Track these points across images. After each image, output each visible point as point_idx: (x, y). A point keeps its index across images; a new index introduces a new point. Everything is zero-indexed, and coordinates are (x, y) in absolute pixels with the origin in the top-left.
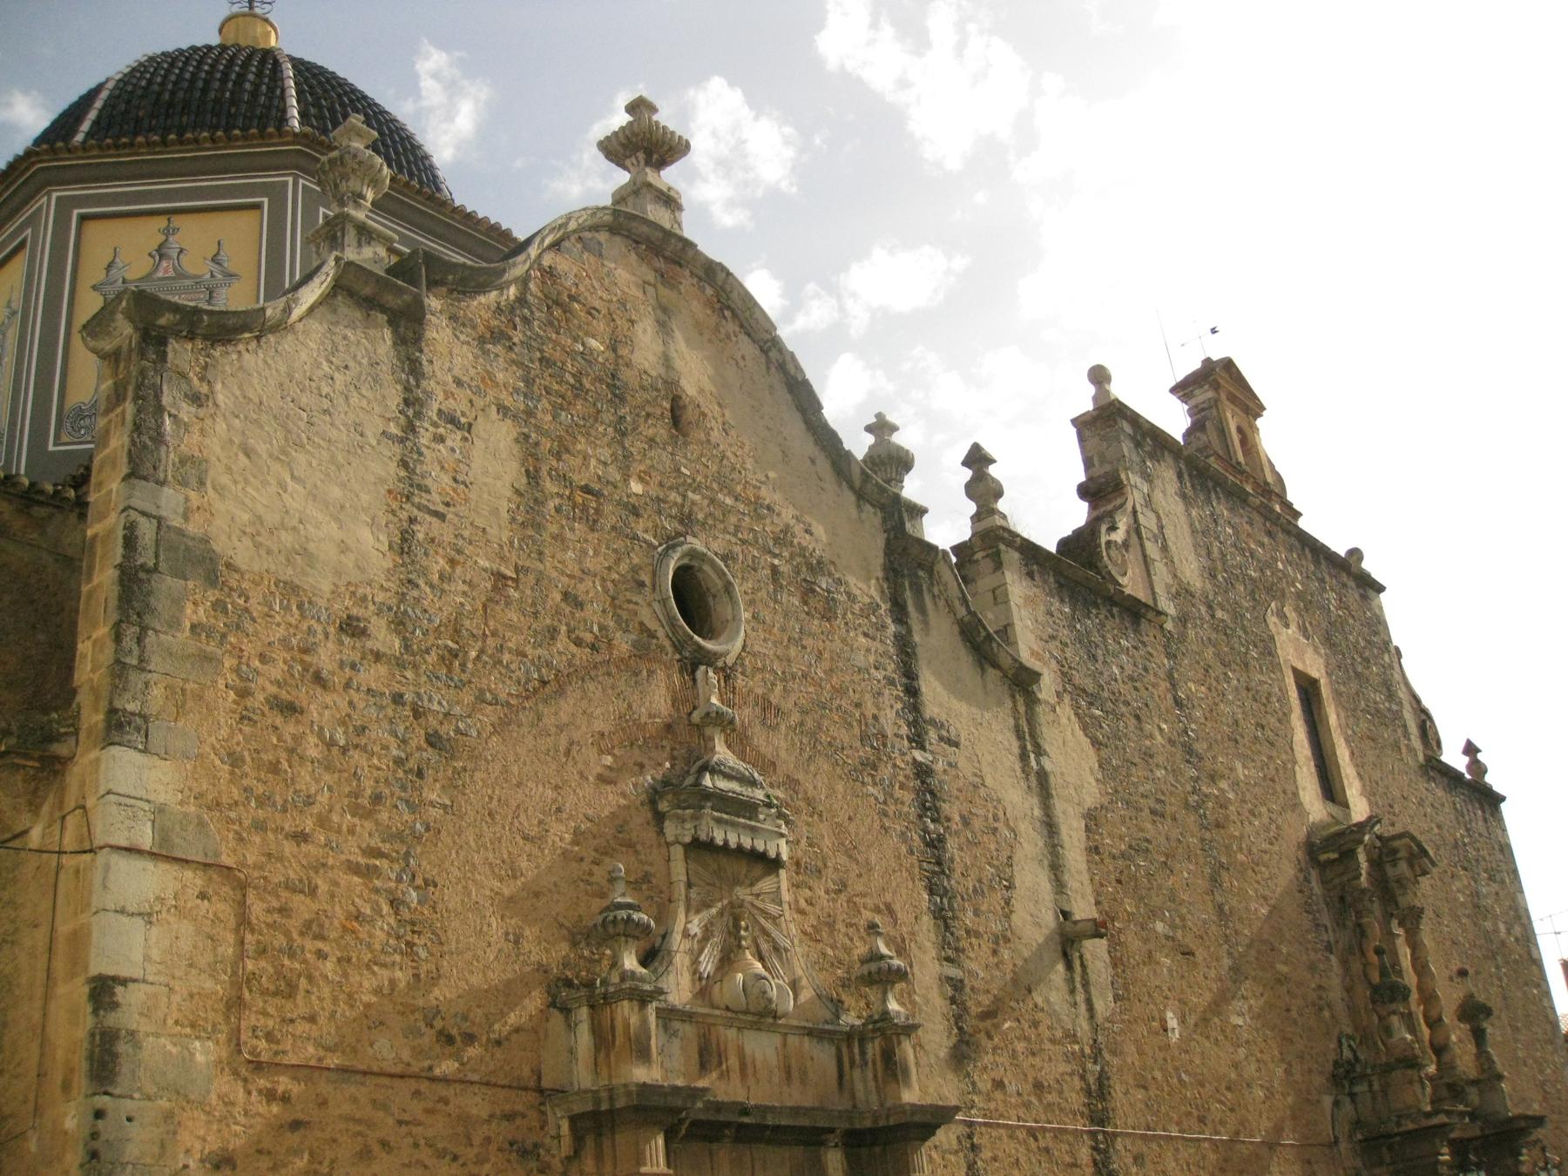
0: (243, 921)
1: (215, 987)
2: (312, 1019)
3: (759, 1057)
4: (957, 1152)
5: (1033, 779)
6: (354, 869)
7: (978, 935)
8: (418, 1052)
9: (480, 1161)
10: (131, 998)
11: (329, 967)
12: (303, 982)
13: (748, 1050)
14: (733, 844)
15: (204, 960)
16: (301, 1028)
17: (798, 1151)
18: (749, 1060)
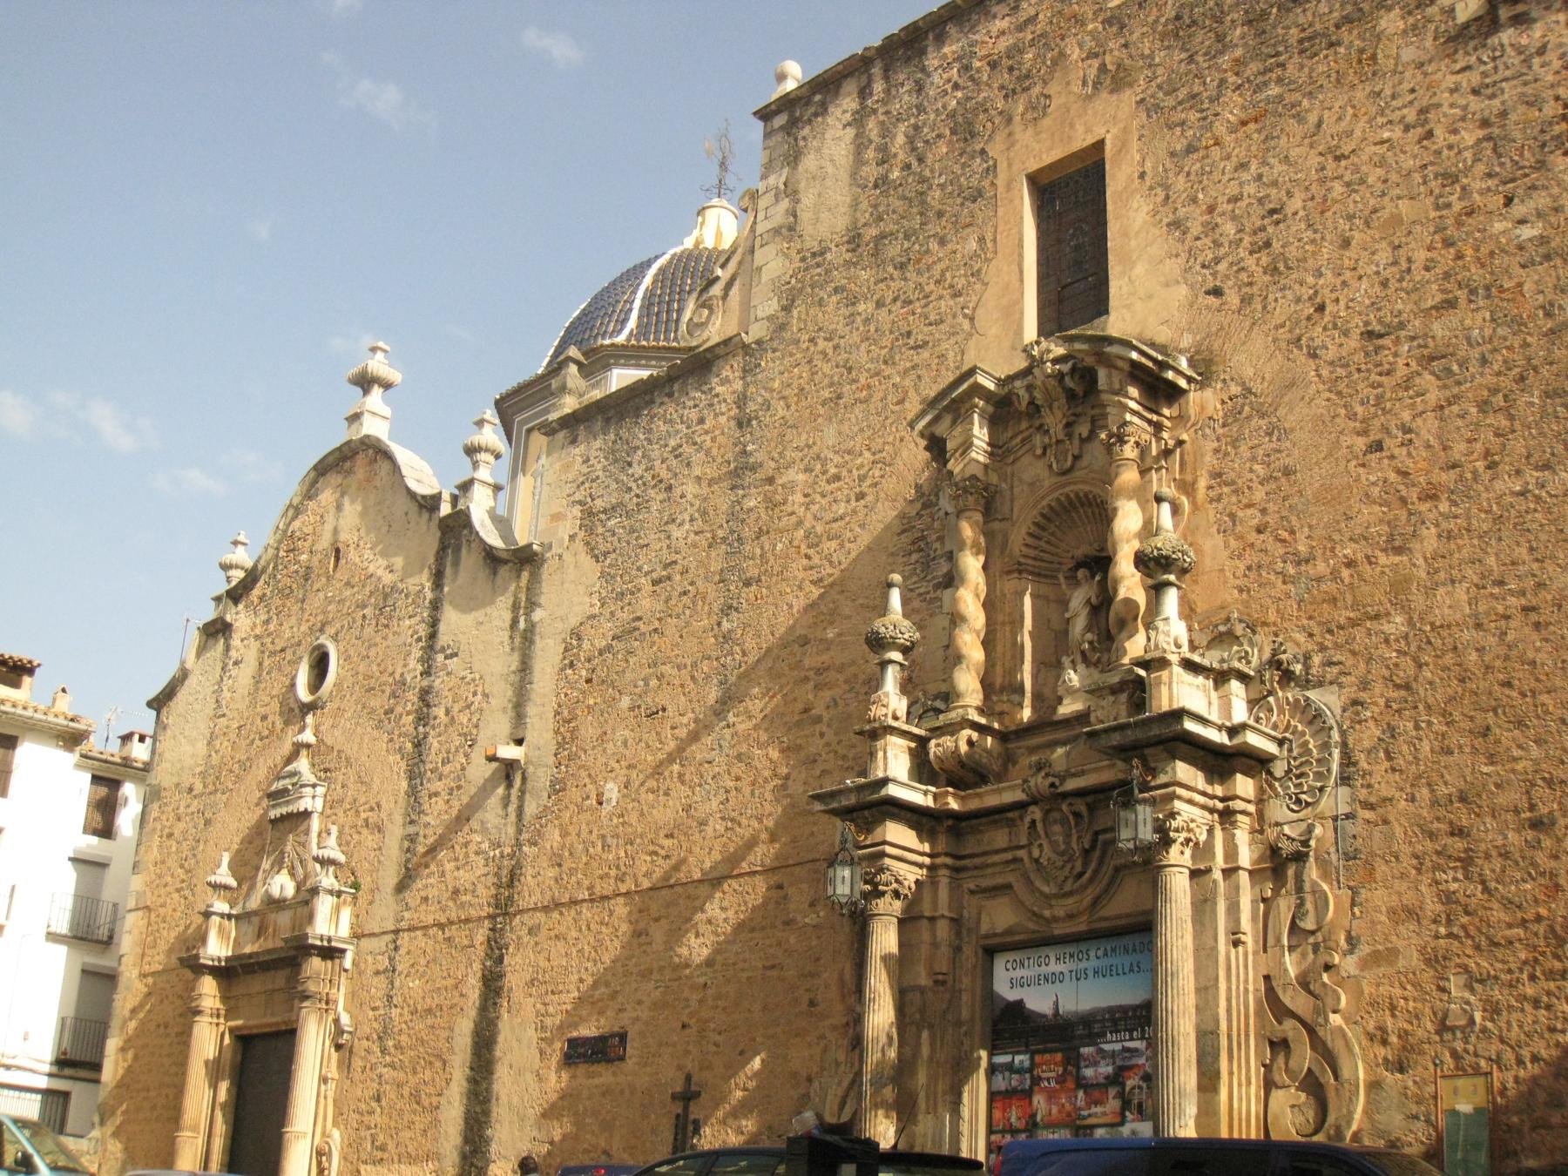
0: (149, 924)
1: (140, 951)
5: (518, 640)
6: (178, 890)
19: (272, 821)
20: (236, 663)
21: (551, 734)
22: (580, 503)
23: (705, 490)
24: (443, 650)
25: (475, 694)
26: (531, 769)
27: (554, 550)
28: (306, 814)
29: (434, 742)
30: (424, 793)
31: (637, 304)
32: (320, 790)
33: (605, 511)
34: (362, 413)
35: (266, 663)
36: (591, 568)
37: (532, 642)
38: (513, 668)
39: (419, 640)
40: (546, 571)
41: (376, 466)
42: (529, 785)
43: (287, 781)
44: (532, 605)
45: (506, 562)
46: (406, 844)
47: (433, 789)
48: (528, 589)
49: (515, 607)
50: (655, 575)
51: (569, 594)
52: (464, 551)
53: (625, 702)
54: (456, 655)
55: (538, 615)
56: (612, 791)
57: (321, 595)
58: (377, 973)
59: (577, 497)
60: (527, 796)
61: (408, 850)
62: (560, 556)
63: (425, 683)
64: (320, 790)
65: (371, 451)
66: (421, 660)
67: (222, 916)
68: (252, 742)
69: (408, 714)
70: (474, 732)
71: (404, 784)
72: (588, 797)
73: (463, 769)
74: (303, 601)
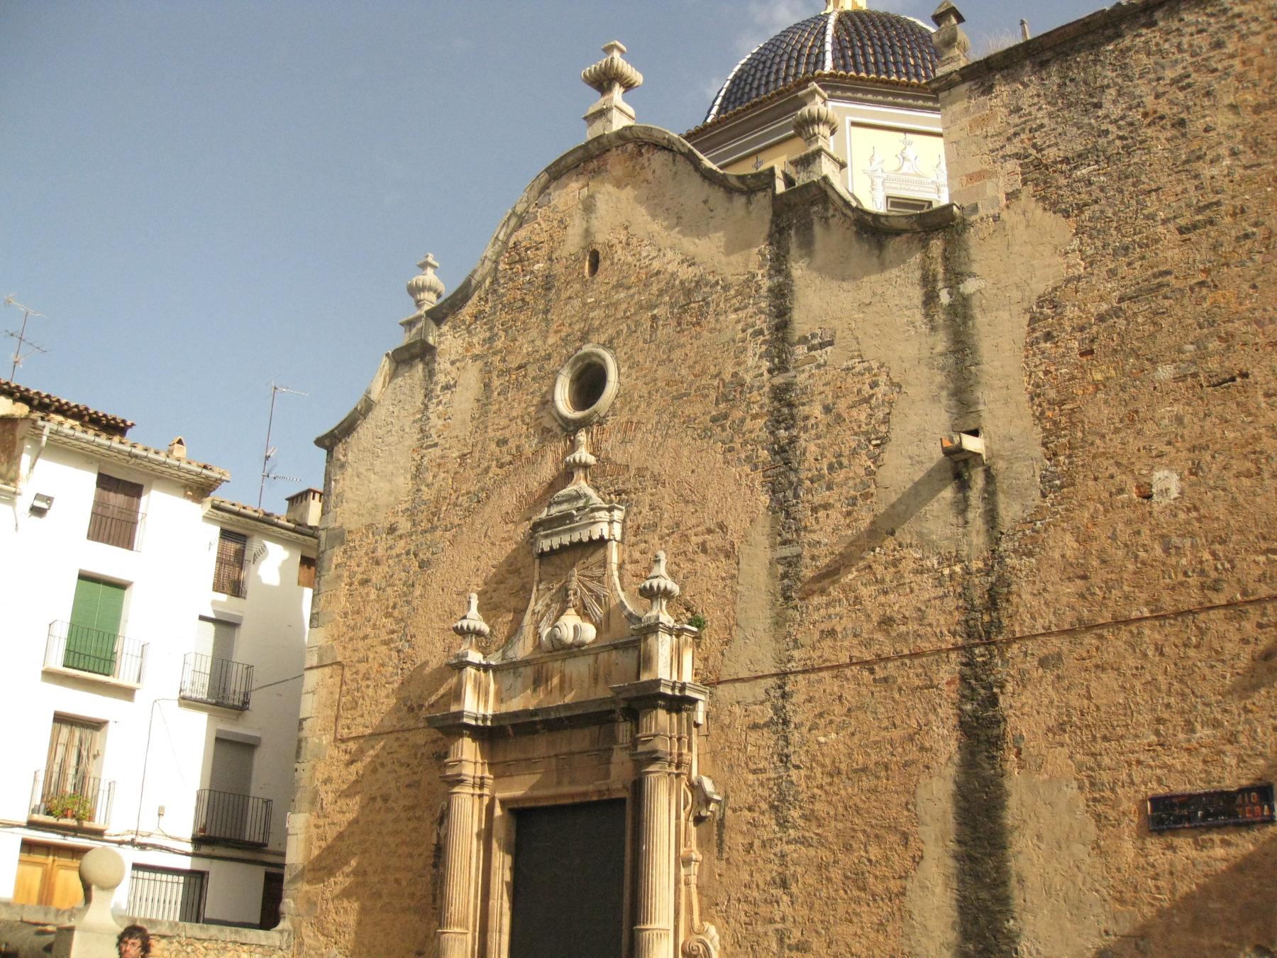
0: (343, 682)
1: (331, 713)
2: (362, 716)
3: (574, 676)
4: (762, 703)
5: (940, 318)
6: (385, 643)
7: (826, 506)
8: (400, 719)
9: (419, 765)
10: (306, 725)
11: (370, 691)
12: (361, 701)
13: (567, 672)
14: (556, 546)
15: (328, 703)
16: (359, 720)
17: (596, 729)
18: (567, 679)
19: (542, 555)
20: (447, 387)
21: (1028, 421)
22: (1017, 156)
23: (1249, 119)
24: (804, 340)
25: (874, 385)
26: (1001, 465)
27: (982, 212)
28: (602, 542)
29: (809, 446)
30: (803, 511)
31: (828, 47)
32: (618, 515)
33: (1066, 160)
34: (609, 109)
35: (496, 383)
36: (1060, 228)
37: (967, 317)
38: (940, 348)
39: (761, 332)
40: (972, 236)
41: (643, 160)
42: (1002, 484)
43: (565, 507)
44: (956, 276)
45: (898, 233)
46: (781, 569)
47: (817, 500)
48: (946, 259)
49: (928, 281)
50: (1181, 222)
51: (1022, 259)
52: (818, 229)
53: (1165, 372)
54: (831, 343)
55: (969, 286)
56: (1167, 481)
57: (577, 303)
58: (755, 727)
59: (1010, 149)
60: (1001, 498)
61: (785, 576)
62: (996, 218)
63: (779, 380)
64: (618, 515)
65: (630, 146)
66: (767, 355)
67: (478, 667)
68: (487, 470)
69: (754, 417)
70: (883, 429)
71: (765, 499)
72: (1121, 491)
73: (870, 473)
74: (546, 312)
